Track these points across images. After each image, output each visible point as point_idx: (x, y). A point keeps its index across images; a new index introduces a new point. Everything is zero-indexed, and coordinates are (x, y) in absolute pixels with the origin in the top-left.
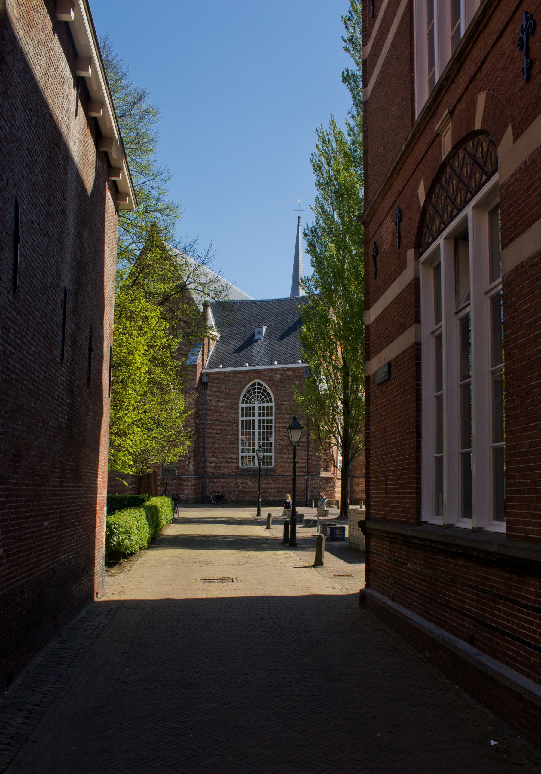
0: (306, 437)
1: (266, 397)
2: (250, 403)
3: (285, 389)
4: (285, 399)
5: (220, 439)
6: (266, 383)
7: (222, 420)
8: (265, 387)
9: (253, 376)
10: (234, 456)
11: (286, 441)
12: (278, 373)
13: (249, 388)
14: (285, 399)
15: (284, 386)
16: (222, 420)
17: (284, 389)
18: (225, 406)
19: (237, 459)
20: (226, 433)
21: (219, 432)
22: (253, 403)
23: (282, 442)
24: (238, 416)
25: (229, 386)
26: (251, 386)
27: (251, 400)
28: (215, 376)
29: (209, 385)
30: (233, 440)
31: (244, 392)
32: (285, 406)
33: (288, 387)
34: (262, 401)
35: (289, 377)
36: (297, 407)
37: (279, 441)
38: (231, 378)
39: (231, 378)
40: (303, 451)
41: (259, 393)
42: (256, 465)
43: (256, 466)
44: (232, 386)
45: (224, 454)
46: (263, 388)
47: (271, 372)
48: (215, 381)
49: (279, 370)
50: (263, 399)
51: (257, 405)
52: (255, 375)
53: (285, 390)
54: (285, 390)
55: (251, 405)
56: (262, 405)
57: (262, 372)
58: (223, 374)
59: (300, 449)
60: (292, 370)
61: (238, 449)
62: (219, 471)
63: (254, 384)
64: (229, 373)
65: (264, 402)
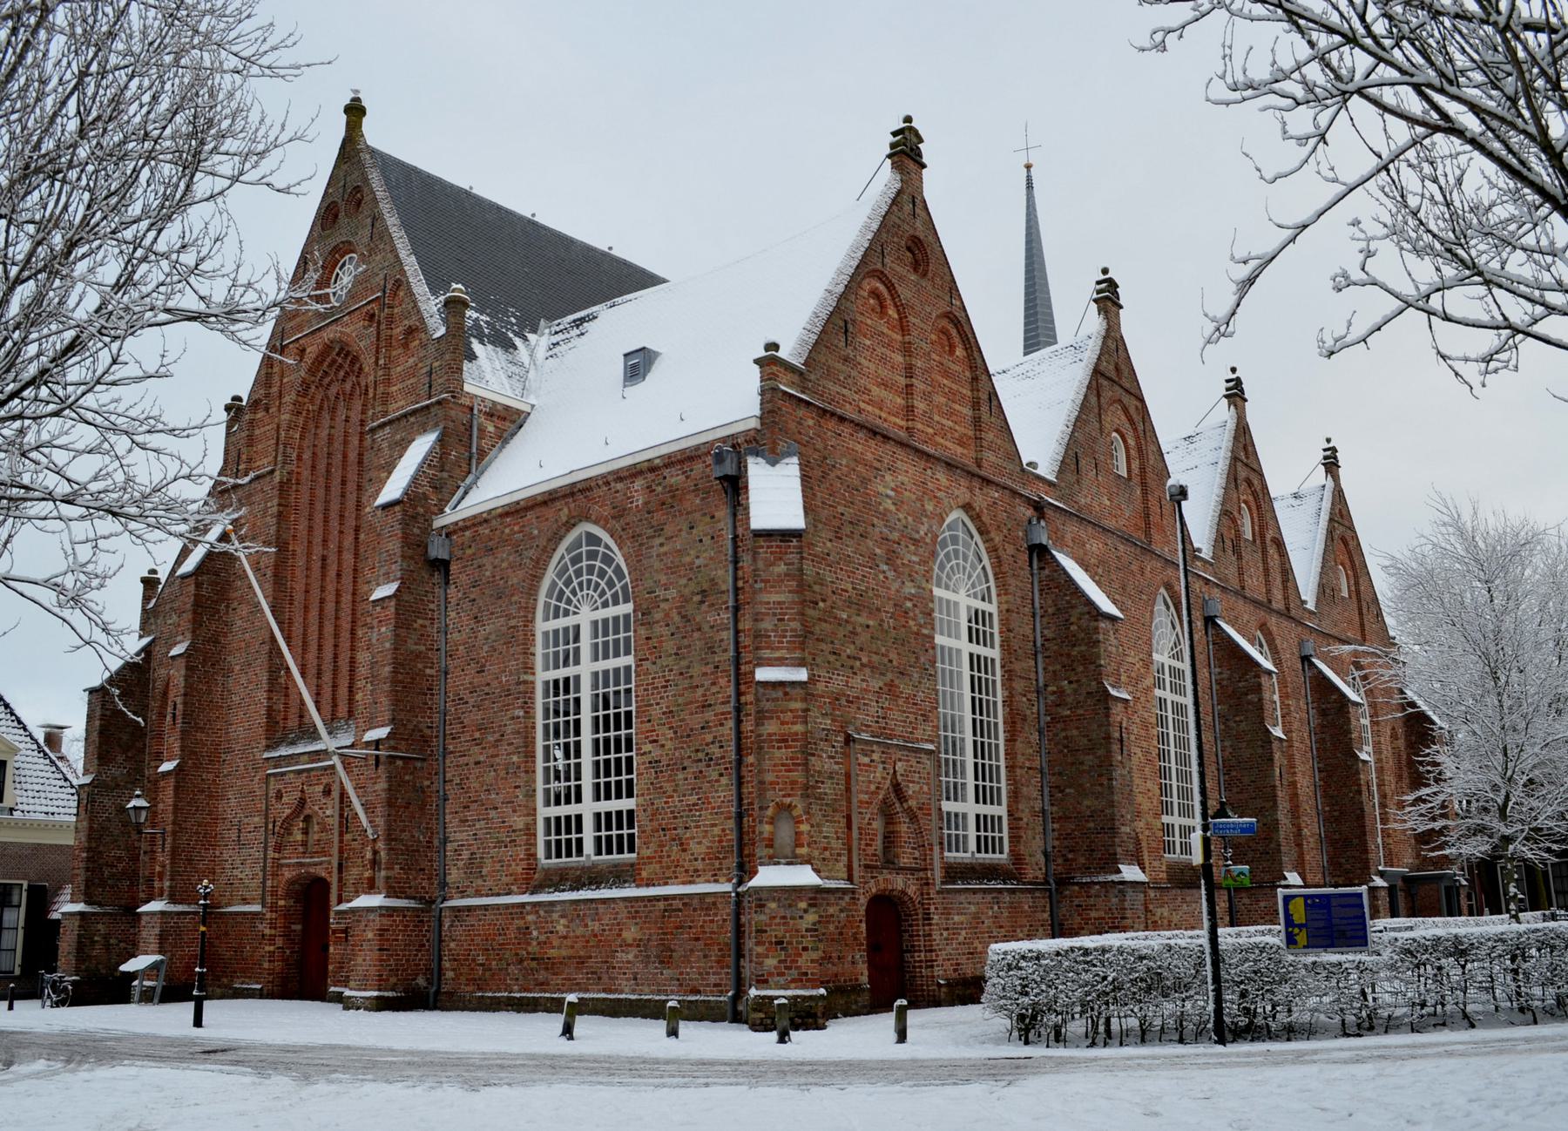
0: (731, 724)
1: (611, 584)
2: (566, 613)
3: (661, 540)
4: (663, 579)
5: (482, 758)
6: (604, 528)
7: (487, 689)
8: (607, 547)
9: (566, 510)
10: (519, 822)
11: (669, 745)
12: (639, 484)
13: (563, 557)
14: (663, 579)
15: (659, 530)
16: (487, 689)
17: (657, 541)
18: (493, 637)
19: (530, 832)
20: (497, 736)
21: (477, 735)
22: (575, 613)
23: (656, 753)
24: (529, 669)
25: (503, 561)
26: (569, 550)
27: (569, 602)
28: (467, 533)
29: (454, 568)
30: (515, 758)
31: (550, 575)
32: (663, 605)
33: (669, 530)
34: (599, 602)
35: (672, 491)
36: (702, 602)
37: (647, 747)
38: (507, 531)
39: (507, 531)
40: (724, 780)
41: (591, 569)
42: (585, 852)
43: (588, 856)
44: (511, 558)
45: (493, 814)
46: (602, 549)
47: (619, 486)
48: (469, 552)
49: (641, 473)
50: (603, 593)
51: (585, 617)
52: (572, 505)
53: (662, 545)
54: (662, 545)
55: (569, 621)
56: (602, 614)
57: (590, 489)
58: (486, 521)
59: (715, 775)
60: (681, 462)
61: (531, 794)
62: (480, 882)
63: (577, 544)
64: (502, 516)
65: (605, 605)
